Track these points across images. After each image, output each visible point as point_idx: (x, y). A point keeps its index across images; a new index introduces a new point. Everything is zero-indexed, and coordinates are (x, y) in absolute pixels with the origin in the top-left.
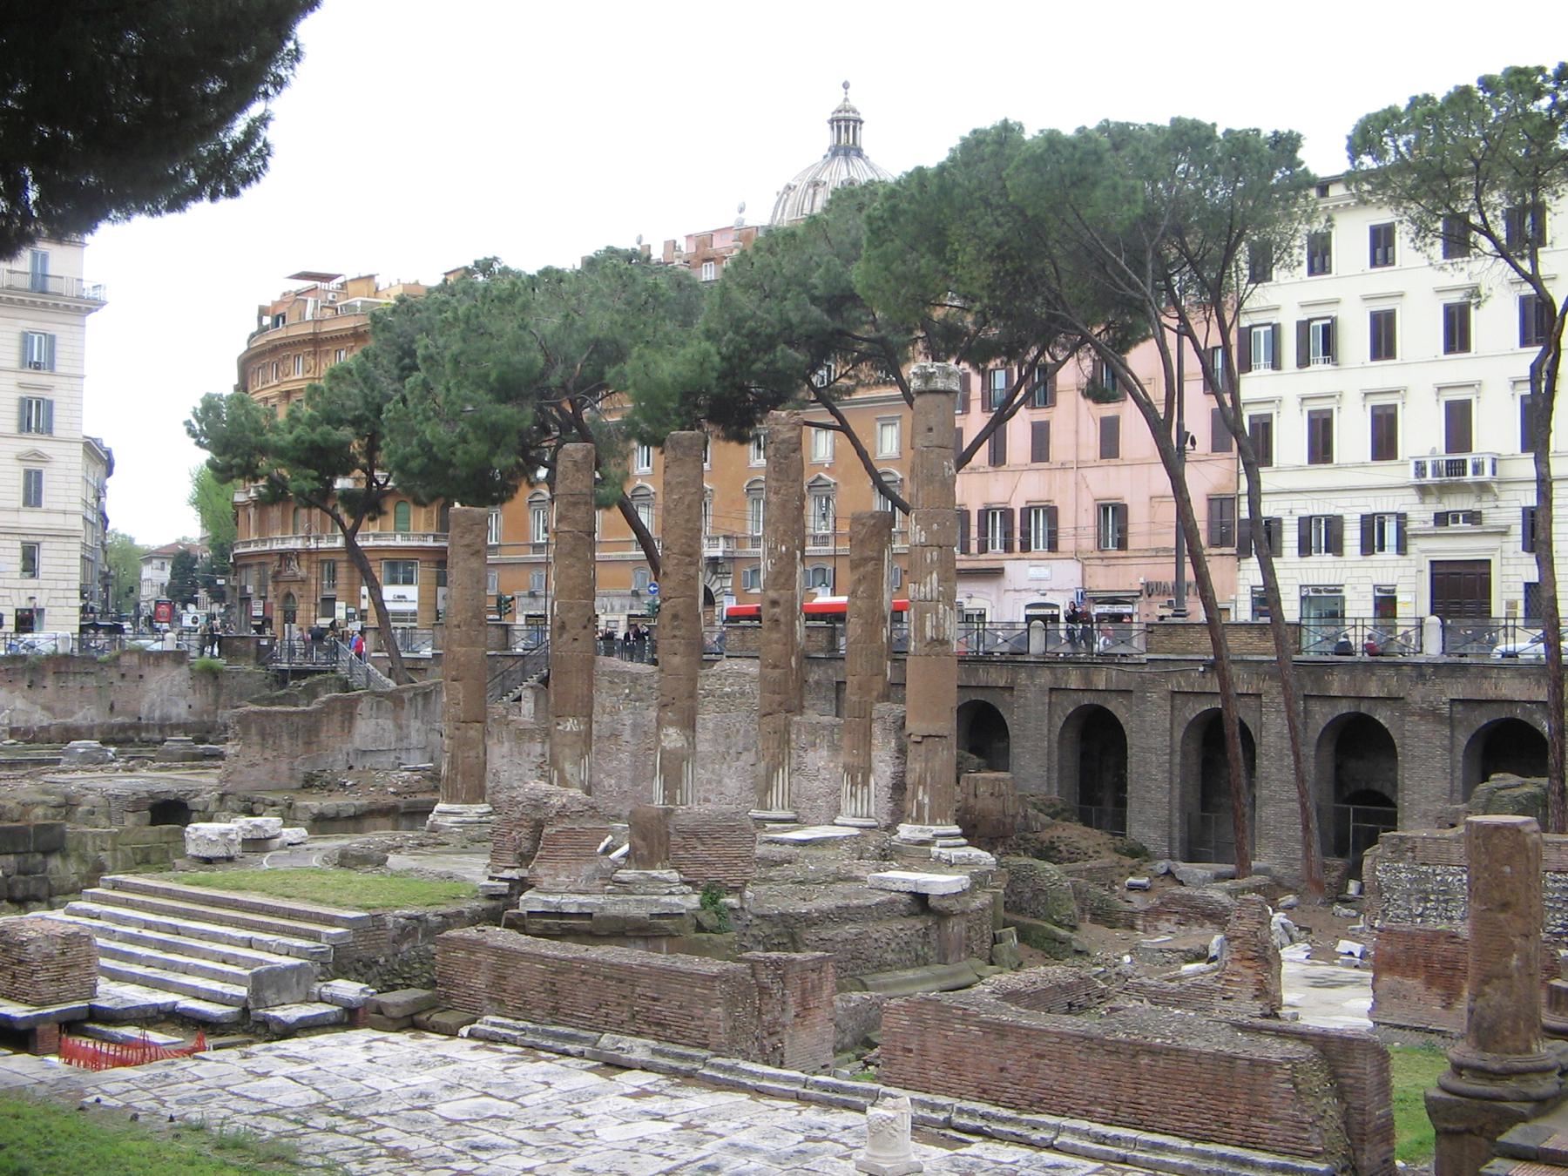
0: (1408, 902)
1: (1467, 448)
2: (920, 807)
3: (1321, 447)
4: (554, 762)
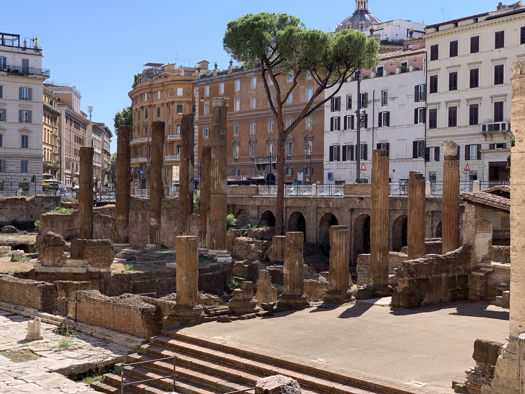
1: (501, 119)
3: (452, 122)
4: (116, 229)
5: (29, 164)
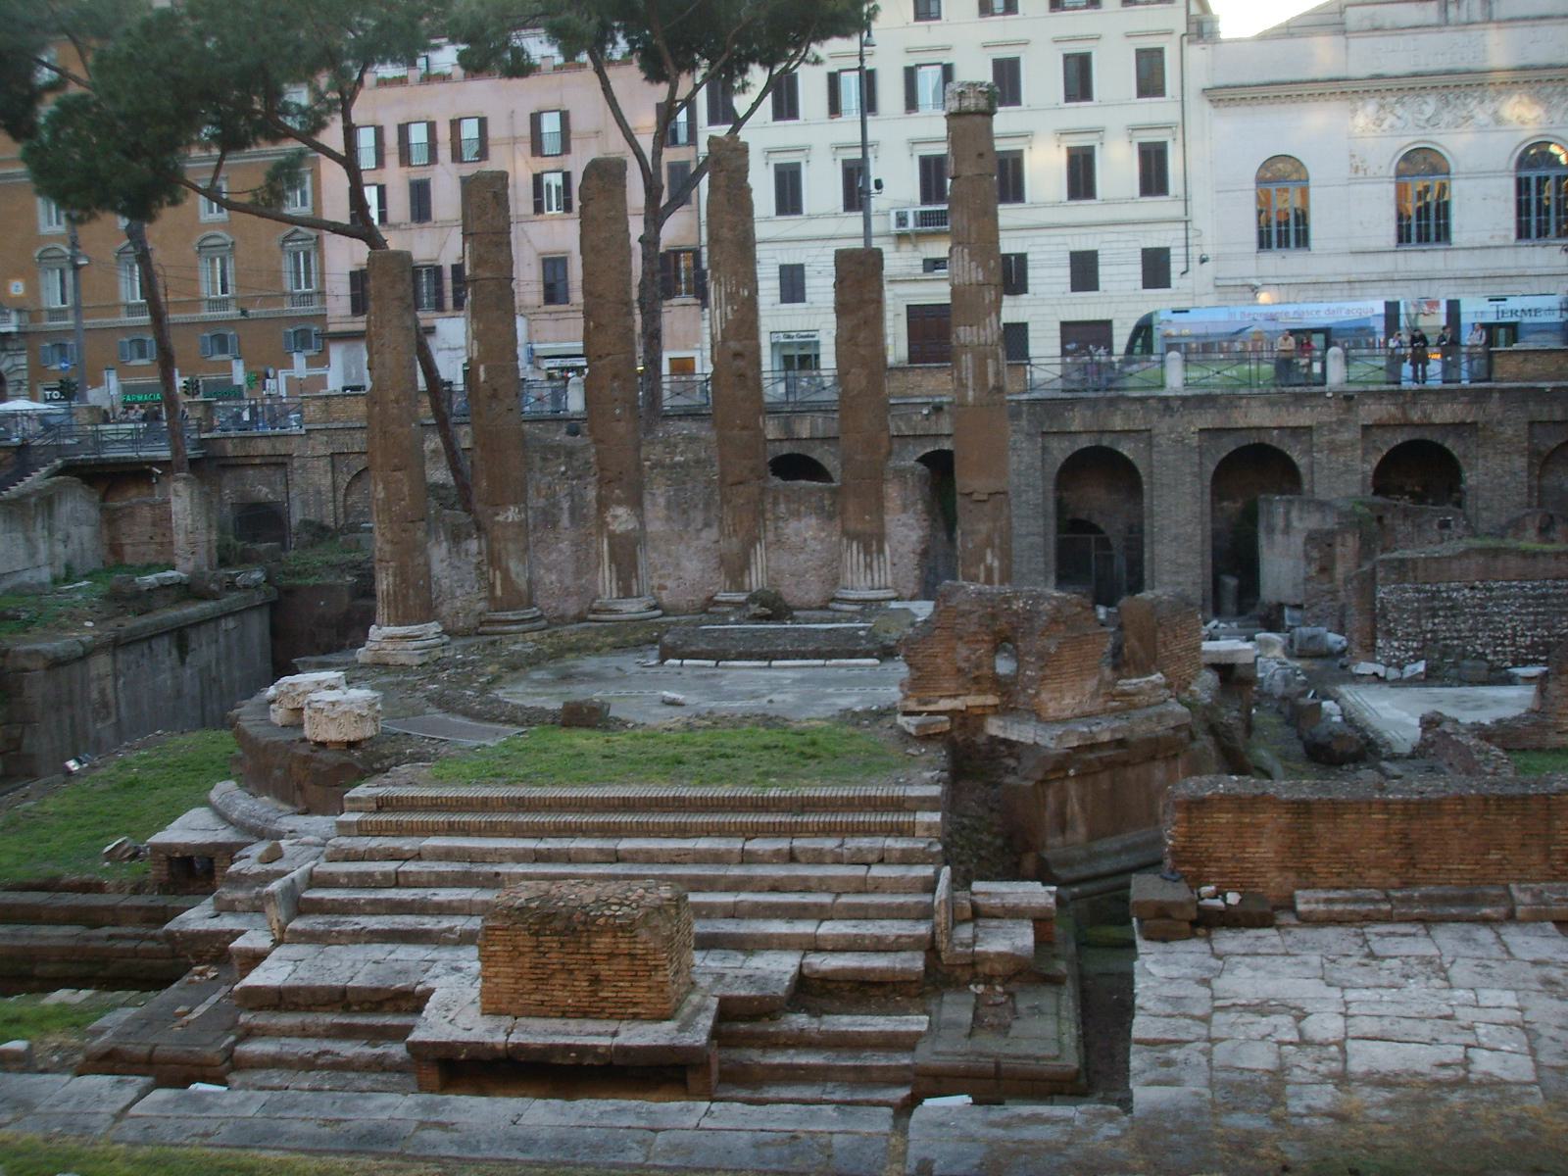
0: (1419, 620)
2: (989, 570)
4: (494, 559)
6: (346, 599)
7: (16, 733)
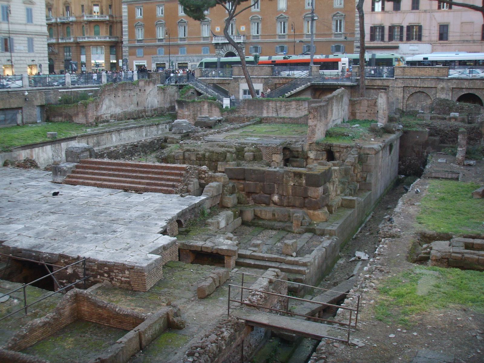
5: (35, 42)
6: (427, 136)
7: (365, 175)
